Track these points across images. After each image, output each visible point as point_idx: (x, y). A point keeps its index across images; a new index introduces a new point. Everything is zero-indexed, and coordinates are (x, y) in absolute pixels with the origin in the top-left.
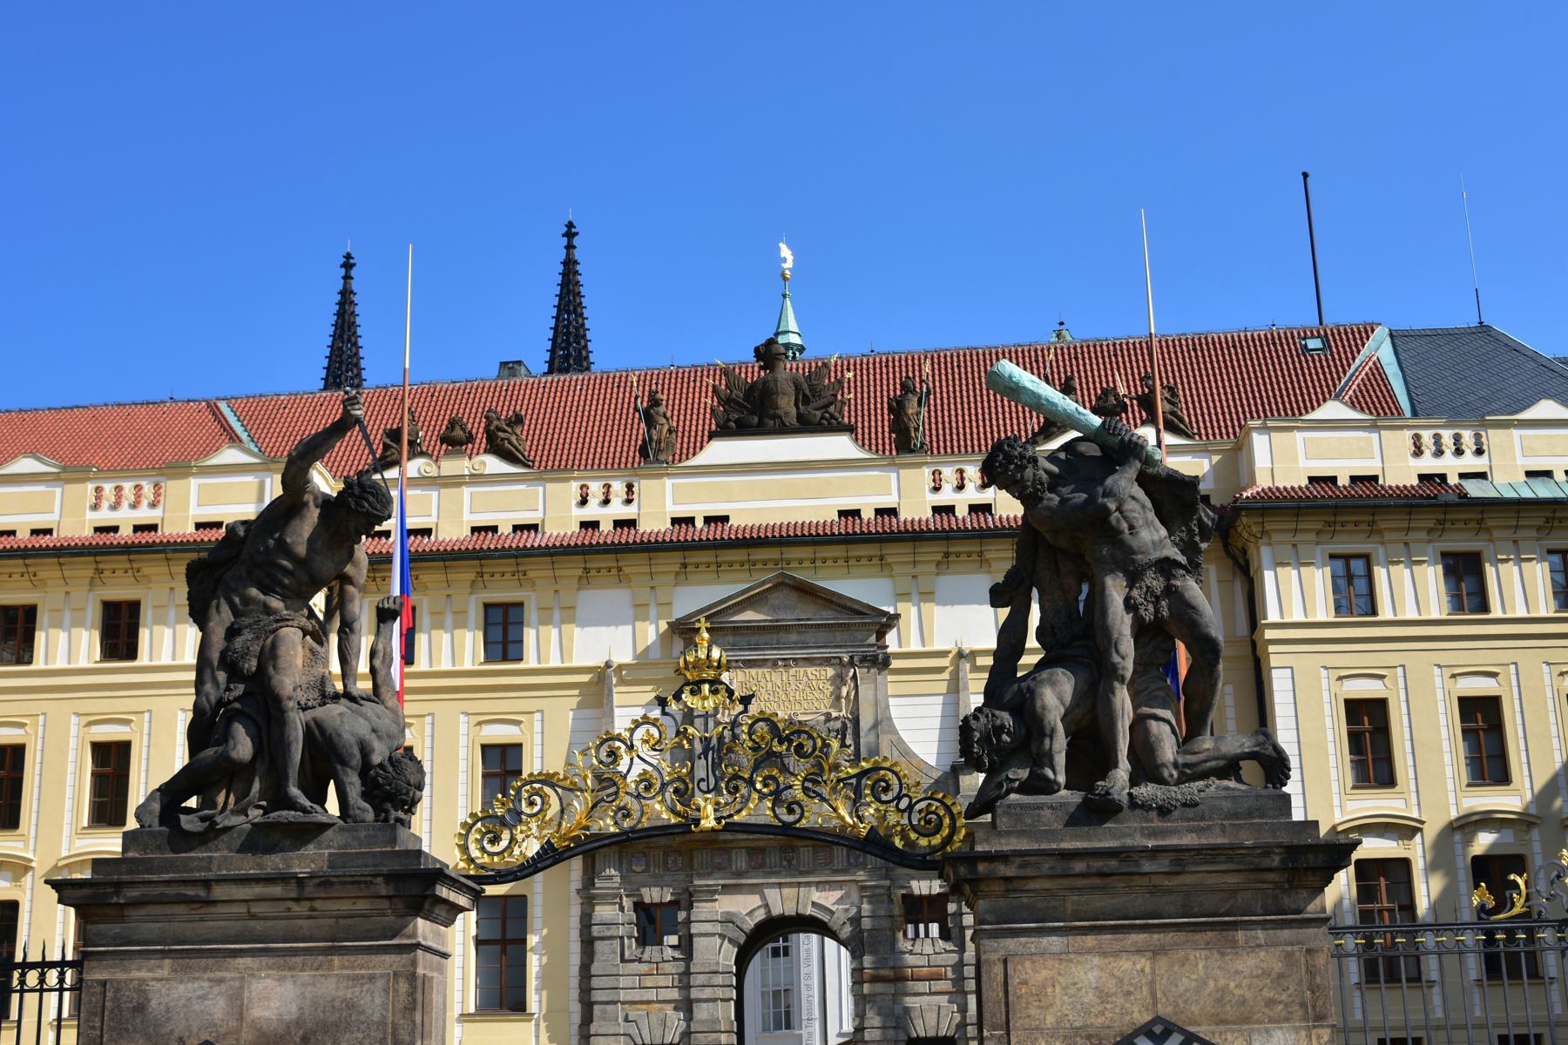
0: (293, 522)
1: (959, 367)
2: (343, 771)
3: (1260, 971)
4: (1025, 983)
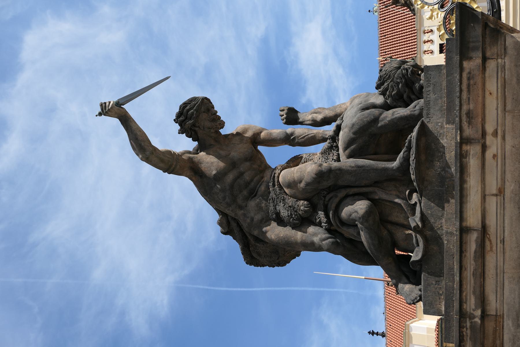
0: (203, 169)
1: (386, 52)
2: (383, 120)
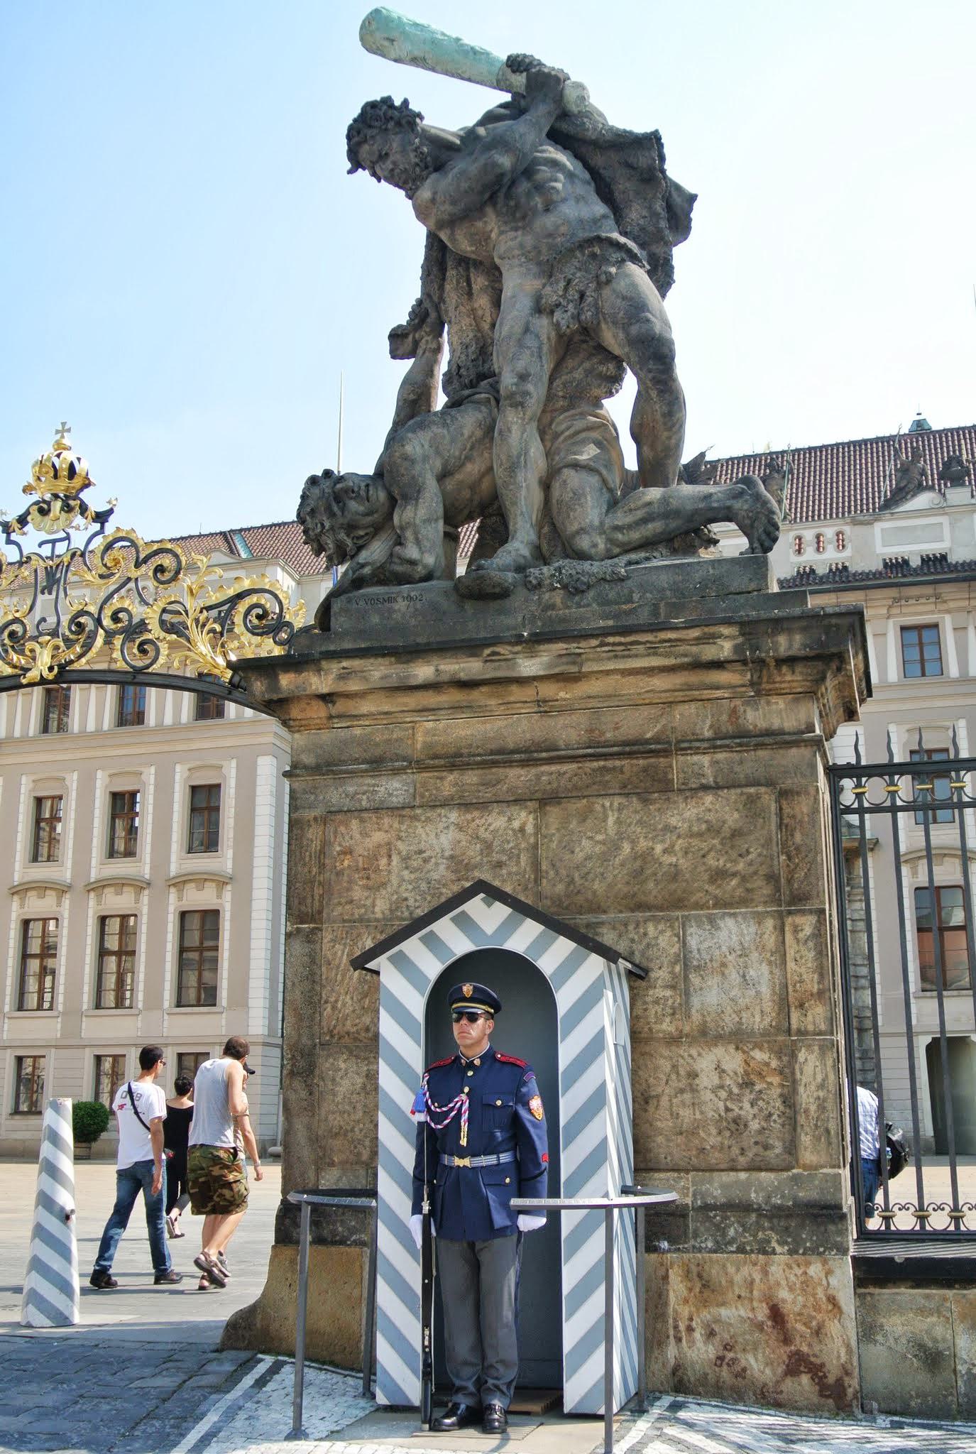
3: (704, 826)
4: (348, 852)
